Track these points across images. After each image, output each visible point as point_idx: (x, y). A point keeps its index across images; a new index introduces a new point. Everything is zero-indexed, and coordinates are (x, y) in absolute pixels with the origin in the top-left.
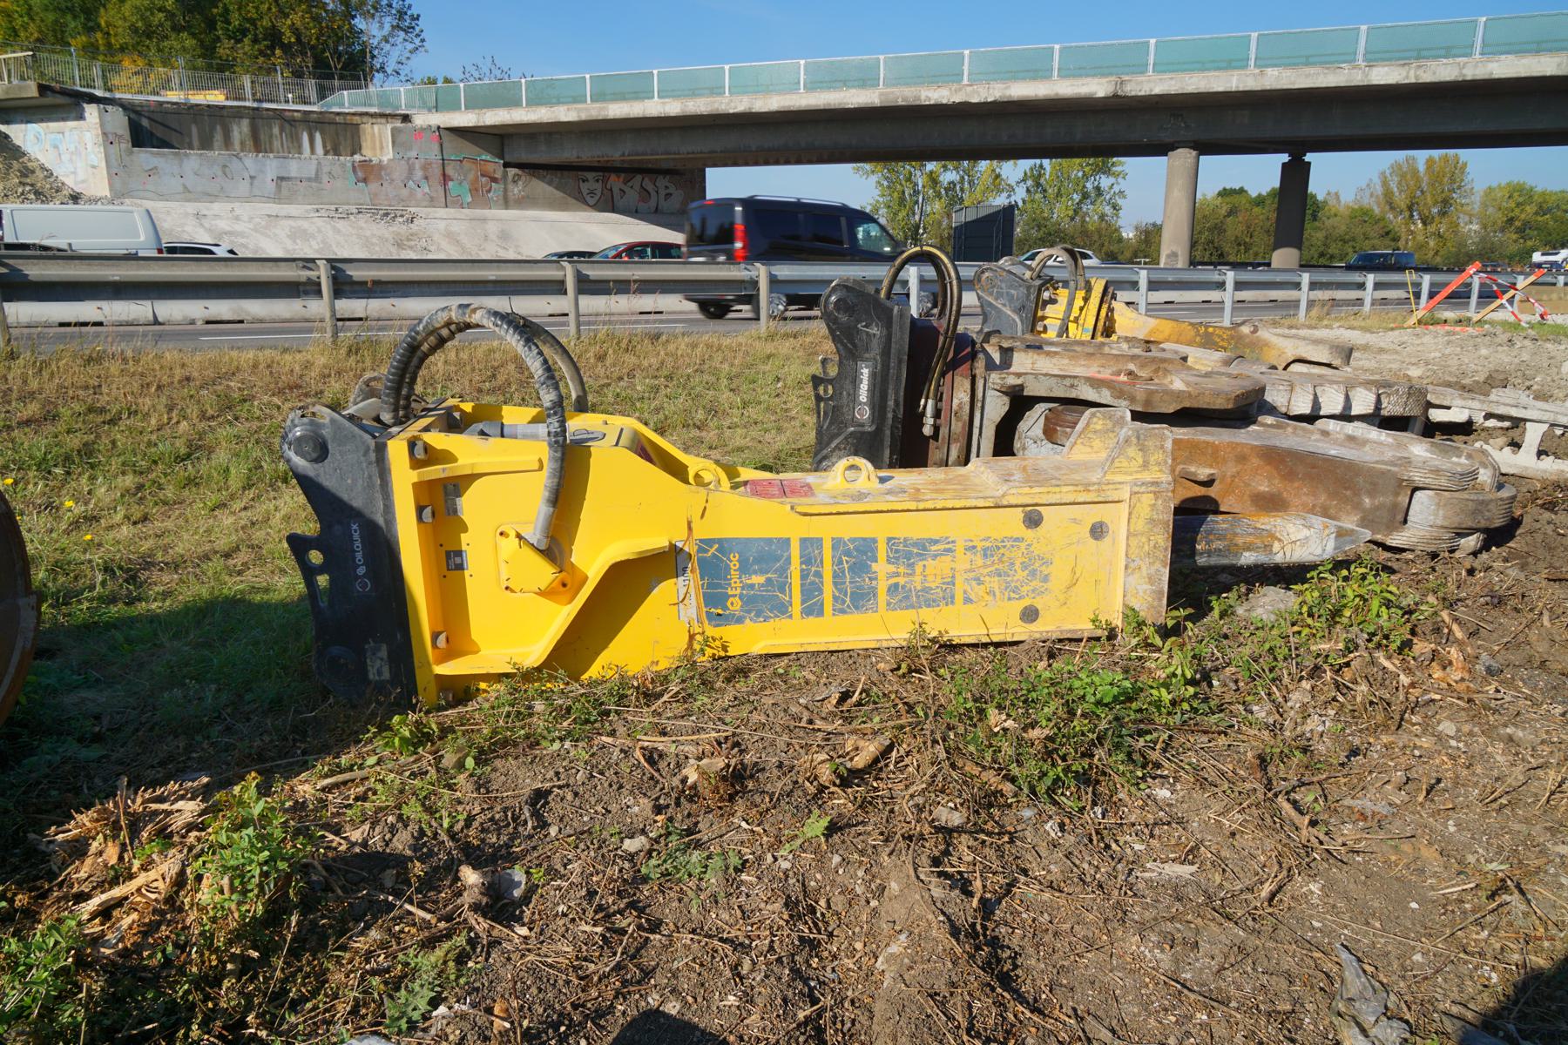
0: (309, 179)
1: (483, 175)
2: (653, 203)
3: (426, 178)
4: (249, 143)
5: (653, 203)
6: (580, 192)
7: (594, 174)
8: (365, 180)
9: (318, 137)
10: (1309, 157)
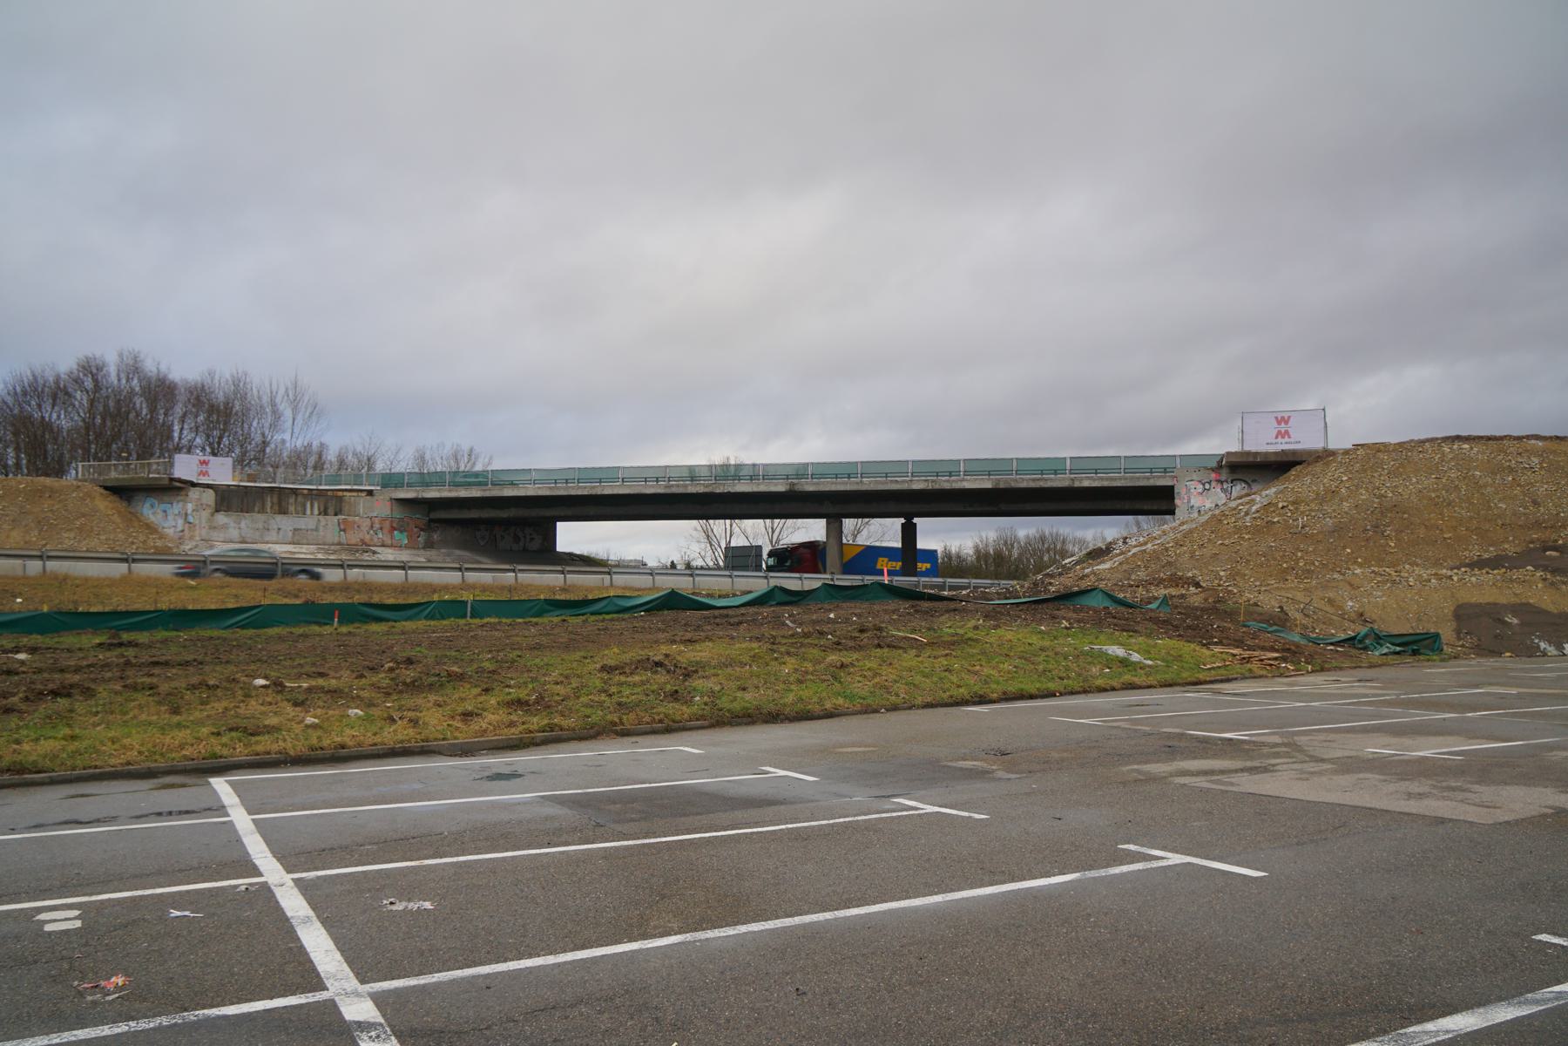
0: (312, 530)
3: (381, 529)
4: (276, 508)
5: (521, 544)
8: (344, 530)
9: (316, 505)
10: (915, 520)
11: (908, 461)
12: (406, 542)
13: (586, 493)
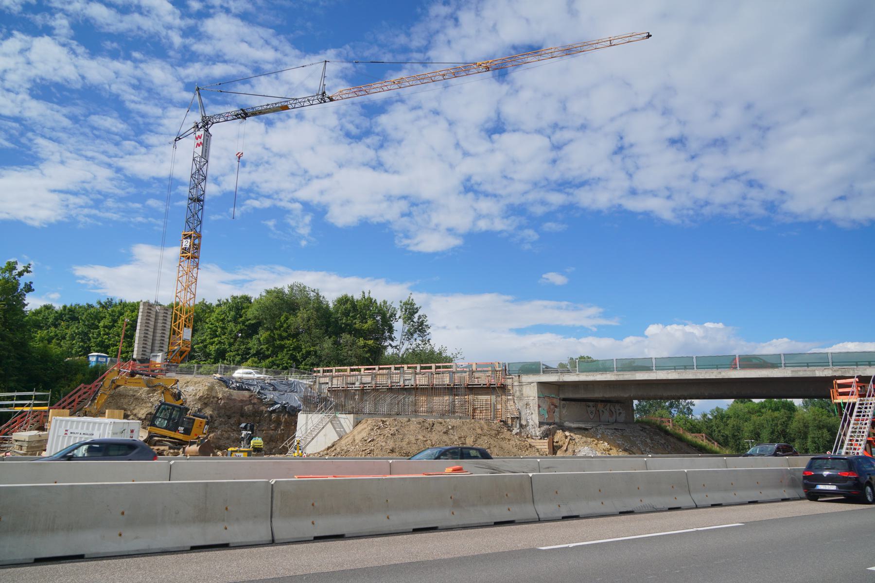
1: (552, 405)
2: (614, 418)
5: (614, 418)
6: (587, 412)
7: (592, 403)
11: (780, 355)
12: (547, 417)
13: (714, 377)
